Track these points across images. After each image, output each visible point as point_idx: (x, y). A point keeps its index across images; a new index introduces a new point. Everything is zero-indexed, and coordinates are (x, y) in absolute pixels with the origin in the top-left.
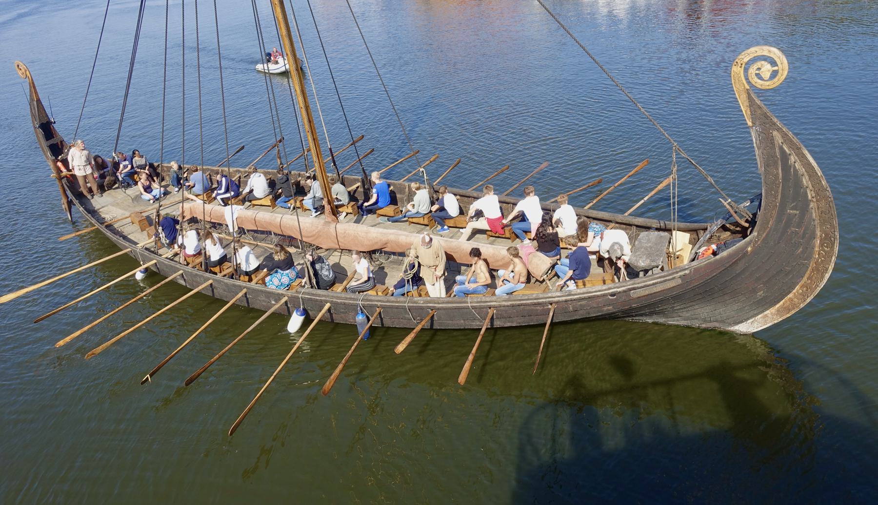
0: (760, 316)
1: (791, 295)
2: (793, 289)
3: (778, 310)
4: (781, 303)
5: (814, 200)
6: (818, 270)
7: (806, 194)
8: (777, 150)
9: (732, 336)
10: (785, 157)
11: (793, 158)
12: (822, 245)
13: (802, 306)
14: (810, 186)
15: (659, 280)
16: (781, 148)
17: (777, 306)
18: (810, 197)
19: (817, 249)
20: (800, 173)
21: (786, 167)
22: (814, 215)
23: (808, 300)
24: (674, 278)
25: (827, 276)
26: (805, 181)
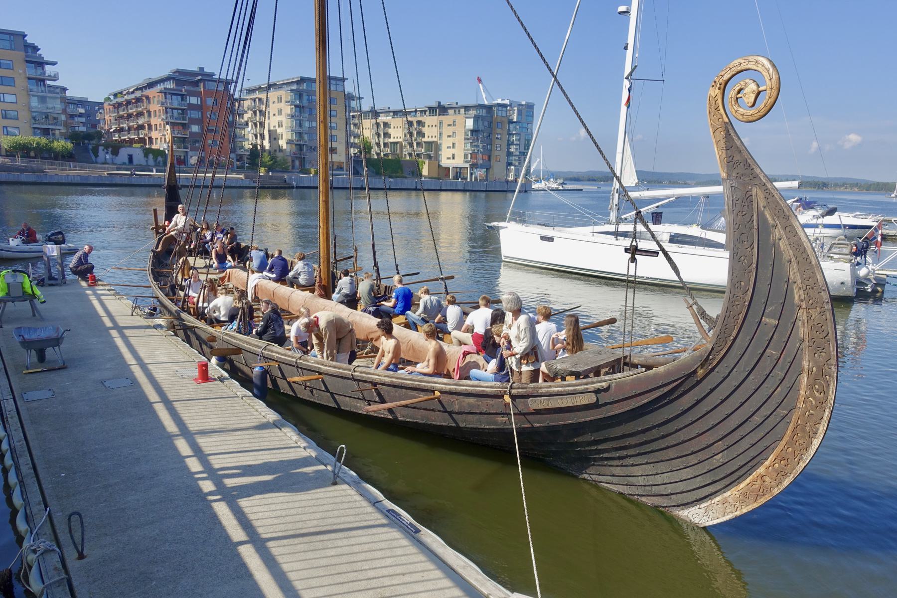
0: (718, 499)
1: (761, 470)
2: (766, 459)
3: (745, 496)
4: (748, 481)
5: (803, 305)
6: (803, 430)
7: (792, 293)
8: (755, 217)
9: (673, 521)
10: (764, 229)
11: (779, 232)
12: (811, 386)
13: (776, 491)
14: (799, 280)
16: (760, 215)
17: (742, 485)
18: (797, 300)
19: (802, 392)
20: (786, 257)
22: (801, 331)
23: (786, 482)
24: (585, 392)
25: (816, 443)
26: (794, 272)
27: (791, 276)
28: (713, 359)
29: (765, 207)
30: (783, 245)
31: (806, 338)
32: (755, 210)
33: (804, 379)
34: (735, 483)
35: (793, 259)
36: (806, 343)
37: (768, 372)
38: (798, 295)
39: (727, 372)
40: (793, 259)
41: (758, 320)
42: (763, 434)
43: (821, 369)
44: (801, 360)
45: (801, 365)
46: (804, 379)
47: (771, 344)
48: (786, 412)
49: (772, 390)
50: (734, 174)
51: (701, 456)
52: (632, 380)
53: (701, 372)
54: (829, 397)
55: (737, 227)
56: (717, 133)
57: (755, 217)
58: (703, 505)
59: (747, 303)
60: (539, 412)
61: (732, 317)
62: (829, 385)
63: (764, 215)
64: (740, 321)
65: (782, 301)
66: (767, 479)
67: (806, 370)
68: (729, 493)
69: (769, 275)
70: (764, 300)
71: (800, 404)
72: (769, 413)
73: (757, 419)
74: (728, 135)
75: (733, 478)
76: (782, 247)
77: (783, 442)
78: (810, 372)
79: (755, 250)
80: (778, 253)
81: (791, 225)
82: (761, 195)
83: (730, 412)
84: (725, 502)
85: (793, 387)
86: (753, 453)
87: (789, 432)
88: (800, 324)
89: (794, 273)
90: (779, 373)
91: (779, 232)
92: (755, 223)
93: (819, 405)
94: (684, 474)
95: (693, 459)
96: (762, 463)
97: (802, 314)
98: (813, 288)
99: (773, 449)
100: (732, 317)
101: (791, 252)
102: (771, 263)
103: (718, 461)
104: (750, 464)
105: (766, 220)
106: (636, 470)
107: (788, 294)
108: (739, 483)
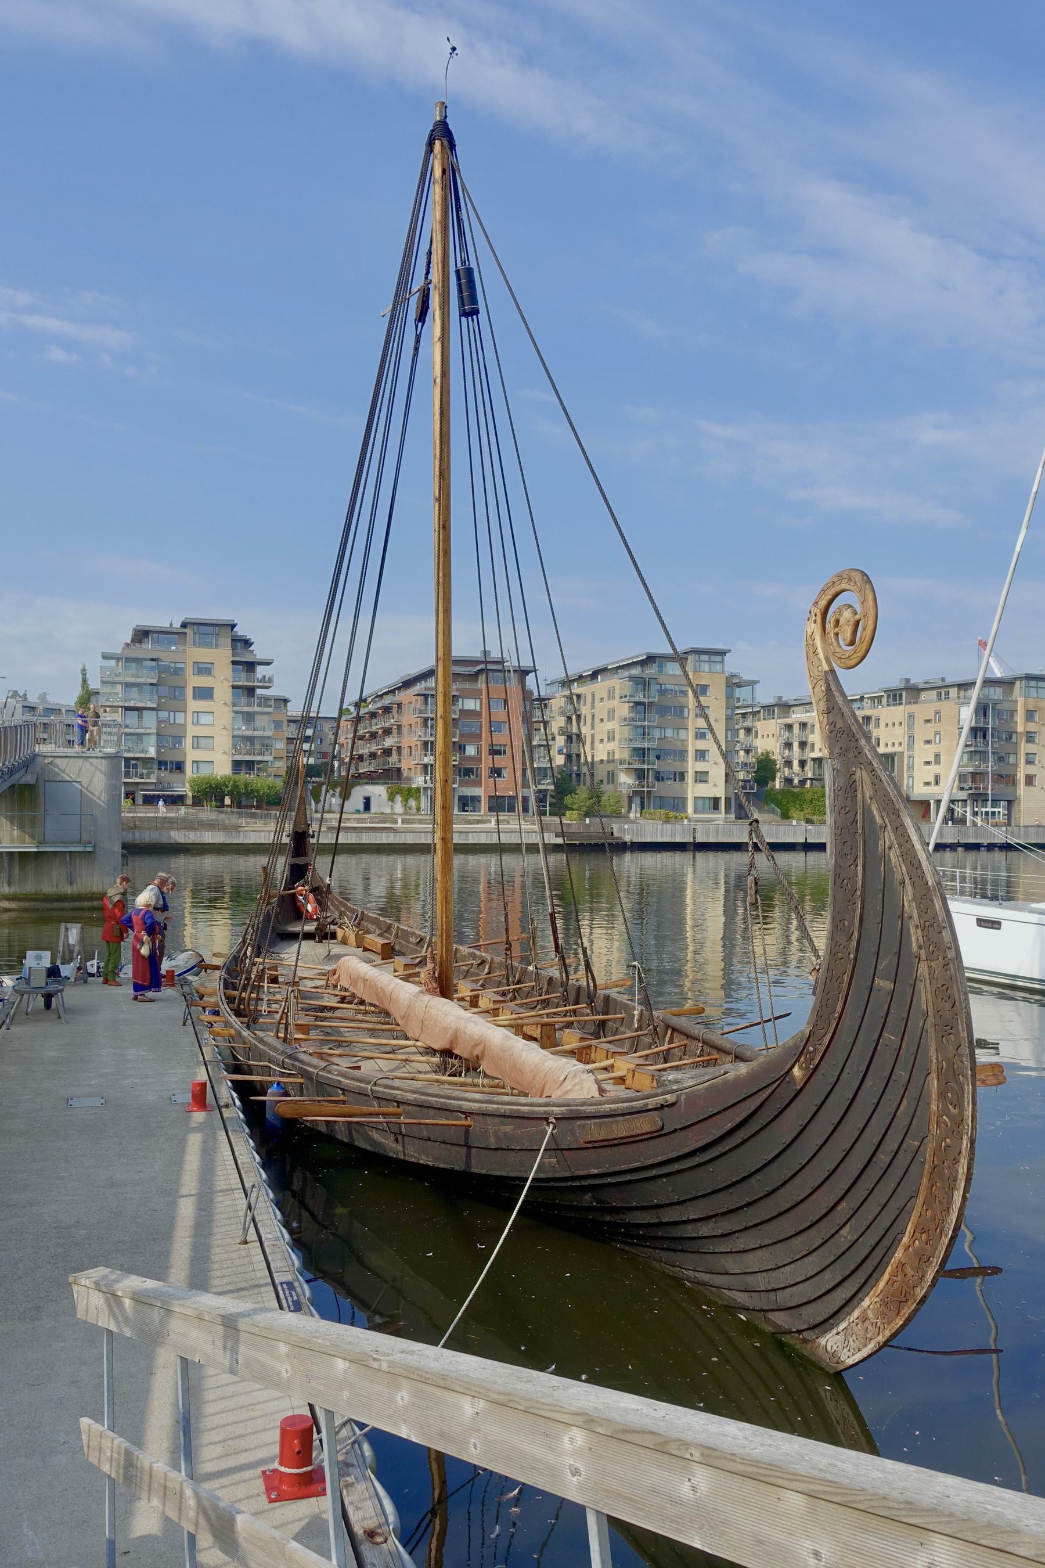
0: (856, 1313)
1: (899, 1254)
3: (885, 1302)
4: (886, 1276)
8: (859, 816)
10: (871, 833)
11: (889, 836)
12: (942, 1095)
14: (915, 914)
15: (626, 1105)
16: (867, 810)
17: (881, 1285)
19: (934, 1107)
20: (898, 877)
21: (875, 860)
22: (924, 1000)
27: (906, 908)
28: (815, 1051)
29: (871, 798)
30: (894, 856)
31: (930, 1009)
32: (860, 803)
33: (934, 1083)
34: (872, 1281)
35: (907, 880)
36: (931, 1021)
37: (887, 1074)
38: (915, 937)
39: (837, 1074)
40: (907, 880)
41: (869, 983)
42: (893, 1185)
43: (951, 1064)
44: (927, 1050)
45: (927, 1059)
46: (934, 1083)
47: (889, 1024)
48: (917, 1143)
49: (895, 1106)
50: (837, 751)
52: (706, 1089)
53: (796, 1071)
54: (966, 1113)
55: (838, 832)
56: (816, 689)
57: (859, 816)
58: (842, 1326)
59: (852, 956)
61: (834, 979)
62: (963, 1090)
63: (871, 811)
64: (845, 986)
65: (896, 950)
66: (908, 1270)
67: (934, 1068)
68: (866, 1303)
69: (879, 907)
70: (875, 950)
72: (896, 1146)
73: (883, 1157)
74: (829, 690)
75: (864, 1270)
76: (893, 861)
77: (920, 1200)
78: (940, 1070)
79: (860, 868)
80: (889, 870)
81: (902, 825)
82: (867, 779)
83: (848, 1146)
84: (864, 1318)
85: (920, 1099)
86: (884, 1222)
87: (925, 1181)
88: (921, 986)
89: (910, 902)
90: (901, 1074)
91: (889, 836)
92: (859, 824)
93: (955, 1127)
94: (811, 1264)
95: (814, 1237)
96: (900, 1241)
97: (923, 969)
98: (932, 925)
99: (910, 1214)
100: (834, 979)
101: (904, 868)
102: (881, 887)
103: (846, 1238)
104: (886, 1242)
105: (872, 818)
106: (752, 1261)
107: (903, 935)
108: (877, 1281)
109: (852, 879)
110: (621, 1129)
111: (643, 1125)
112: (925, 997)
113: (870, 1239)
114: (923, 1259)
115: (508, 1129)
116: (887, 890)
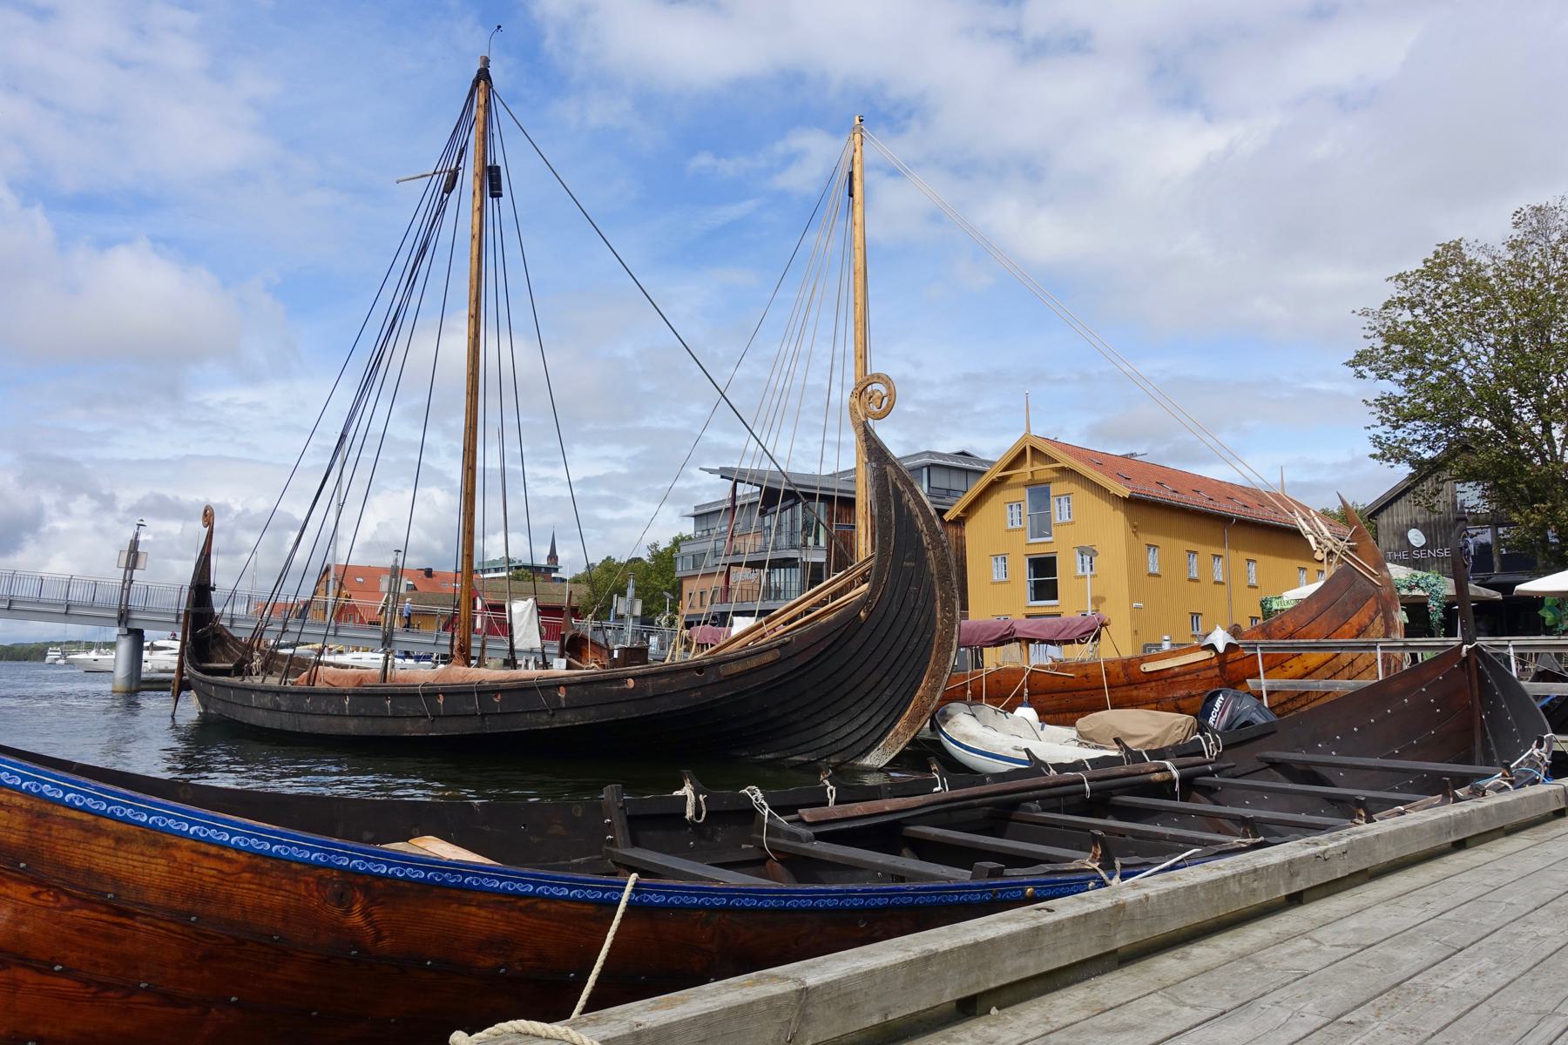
1: (920, 692)
3: (910, 720)
10: (898, 495)
11: (907, 496)
12: (943, 609)
16: (895, 485)
21: (900, 506)
26: (920, 522)
30: (912, 504)
38: (926, 540)
51: (873, 695)
60: (732, 677)
71: (939, 627)
73: (911, 648)
84: (897, 733)
85: (932, 614)
95: (867, 701)
109: (889, 518)
110: (753, 663)
111: (769, 657)
112: (933, 567)
113: (903, 691)
114: (934, 689)
115: (665, 681)
116: (911, 518)
